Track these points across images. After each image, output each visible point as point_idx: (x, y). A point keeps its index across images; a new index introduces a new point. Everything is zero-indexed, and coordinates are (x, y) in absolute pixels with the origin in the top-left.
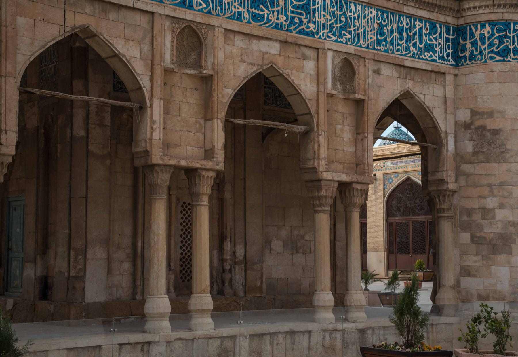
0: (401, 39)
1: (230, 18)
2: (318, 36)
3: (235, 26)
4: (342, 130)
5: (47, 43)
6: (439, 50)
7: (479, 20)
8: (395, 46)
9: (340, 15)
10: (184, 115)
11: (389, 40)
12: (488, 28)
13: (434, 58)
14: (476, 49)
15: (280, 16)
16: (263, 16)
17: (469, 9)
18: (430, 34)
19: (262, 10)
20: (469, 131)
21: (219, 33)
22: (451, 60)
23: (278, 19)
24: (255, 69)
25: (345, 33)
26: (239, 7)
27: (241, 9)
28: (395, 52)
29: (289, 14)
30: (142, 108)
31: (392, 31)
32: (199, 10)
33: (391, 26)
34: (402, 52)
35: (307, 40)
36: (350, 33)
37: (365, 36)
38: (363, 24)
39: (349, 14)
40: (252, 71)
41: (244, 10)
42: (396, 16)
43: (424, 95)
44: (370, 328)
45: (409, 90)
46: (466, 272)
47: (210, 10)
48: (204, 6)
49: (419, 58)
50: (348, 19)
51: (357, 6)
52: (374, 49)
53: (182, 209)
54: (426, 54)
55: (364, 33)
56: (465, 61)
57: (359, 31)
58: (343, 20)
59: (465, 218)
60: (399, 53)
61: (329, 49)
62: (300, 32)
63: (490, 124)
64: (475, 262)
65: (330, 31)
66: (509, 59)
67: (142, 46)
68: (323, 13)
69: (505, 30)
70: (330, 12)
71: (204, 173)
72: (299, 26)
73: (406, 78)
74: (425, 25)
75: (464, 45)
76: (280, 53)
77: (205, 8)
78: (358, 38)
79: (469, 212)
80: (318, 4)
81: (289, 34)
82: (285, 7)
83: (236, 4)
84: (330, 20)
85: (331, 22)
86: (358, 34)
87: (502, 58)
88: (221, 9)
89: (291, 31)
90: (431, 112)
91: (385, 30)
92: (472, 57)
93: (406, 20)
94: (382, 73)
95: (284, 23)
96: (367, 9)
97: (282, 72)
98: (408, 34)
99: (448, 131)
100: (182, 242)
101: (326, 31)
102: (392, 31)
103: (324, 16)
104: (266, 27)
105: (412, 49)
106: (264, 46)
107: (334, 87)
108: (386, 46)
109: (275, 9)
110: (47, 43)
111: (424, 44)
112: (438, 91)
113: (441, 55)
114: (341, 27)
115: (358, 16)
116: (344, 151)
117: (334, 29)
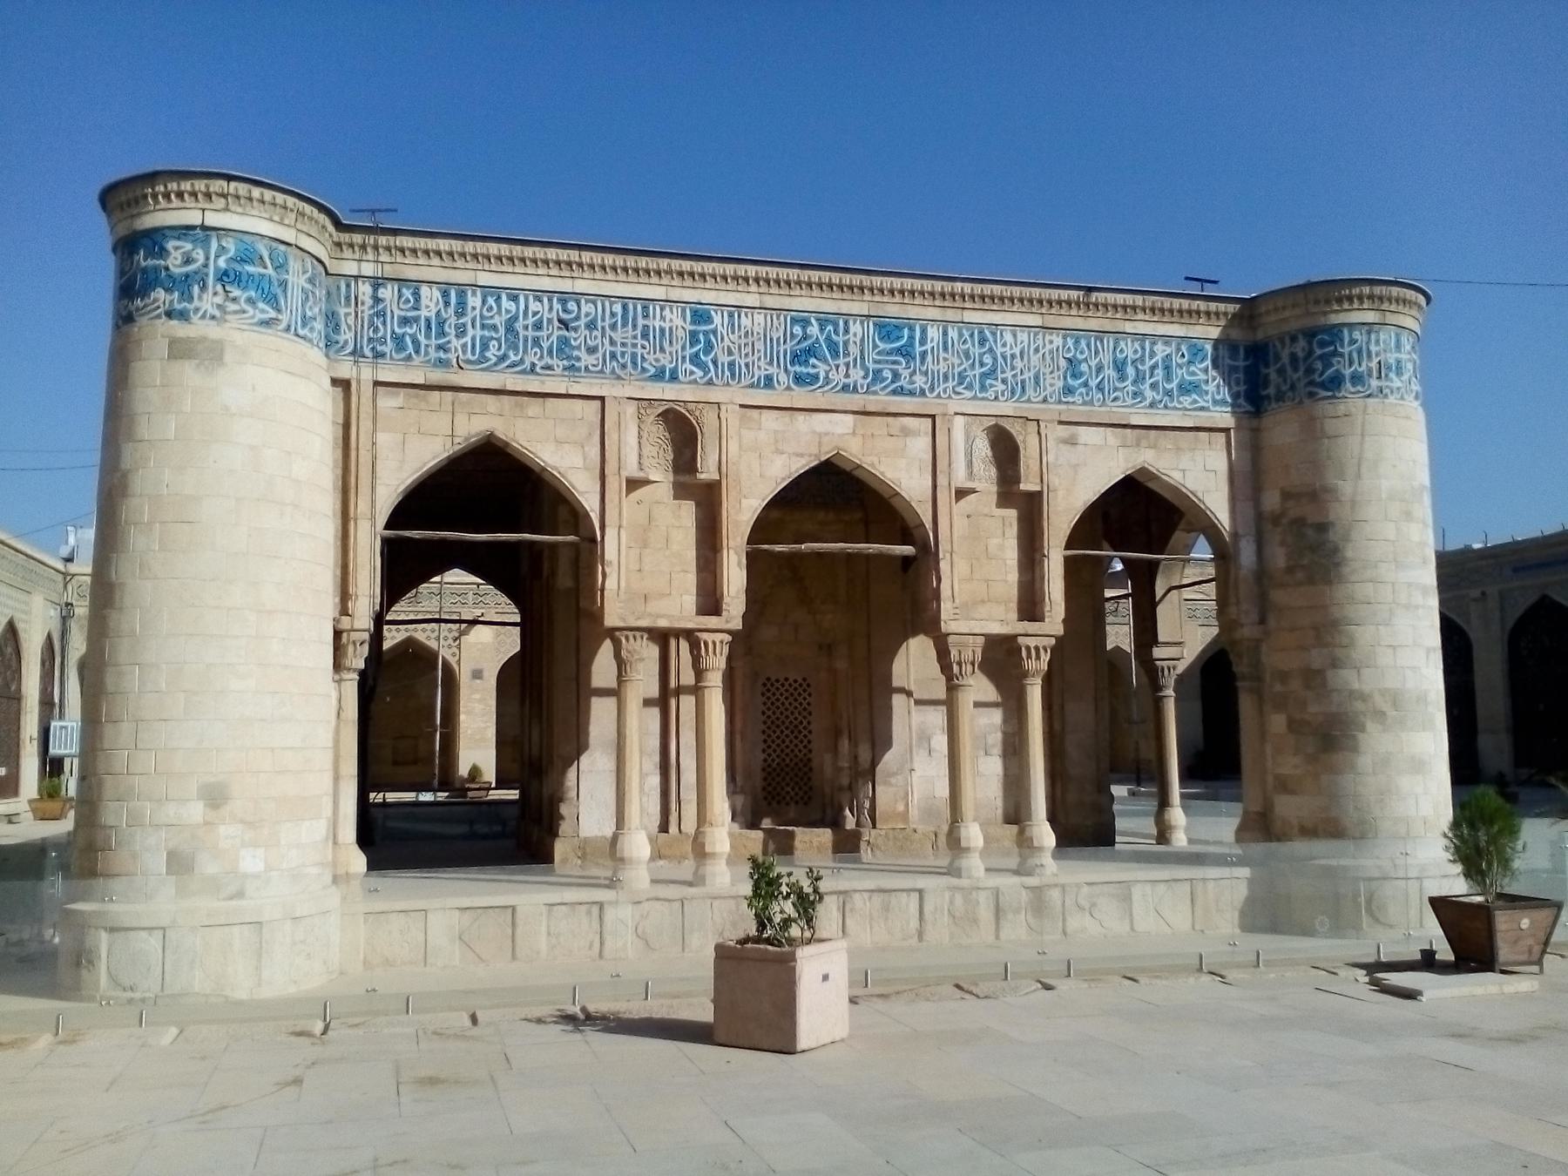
0: (1122, 378)
1: (752, 386)
2: (935, 394)
3: (761, 397)
4: (1001, 547)
5: (425, 464)
6: (1215, 389)
7: (1286, 328)
8: (1109, 393)
9: (981, 355)
10: (675, 547)
11: (1093, 383)
12: (1302, 342)
13: (1203, 404)
14: (1285, 381)
15: (851, 371)
16: (816, 377)
17: (1268, 312)
18: (1190, 362)
19: (814, 366)
20: (1279, 529)
22: (1244, 403)
23: (847, 376)
24: (803, 461)
25: (994, 382)
26: (767, 367)
27: (773, 370)
28: (1108, 402)
29: (871, 366)
31: (1100, 369)
32: (690, 383)
33: (1098, 360)
34: (1124, 401)
36: (1004, 381)
37: (1037, 383)
38: (1032, 364)
39: (999, 350)
40: (799, 465)
41: (778, 371)
42: (1108, 342)
43: (1184, 471)
44: (1056, 885)
45: (1146, 466)
46: (1284, 786)
47: (711, 379)
48: (701, 373)
49: (1166, 407)
50: (1000, 359)
51: (1019, 334)
52: (1060, 402)
53: (764, 690)
54: (1181, 399)
55: (1037, 378)
56: (1270, 403)
57: (1026, 376)
58: (988, 359)
59: (1278, 688)
60: (1119, 403)
61: (956, 414)
62: (894, 392)
64: (1296, 767)
65: (960, 384)
66: (1343, 393)
67: (586, 449)
68: (942, 355)
69: (1332, 343)
70: (958, 352)
71: (704, 636)
72: (893, 382)
73: (1138, 445)
74: (1178, 349)
75: (1267, 375)
76: (854, 431)
77: (700, 378)
78: (1023, 388)
79: (1284, 677)
80: (932, 341)
81: (872, 397)
82: (862, 352)
83: (762, 363)
84: (959, 365)
85: (963, 367)
86: (1023, 382)
87: (1330, 394)
88: (733, 375)
89: (875, 393)
90: (1199, 500)
91: (1084, 367)
92: (1280, 397)
93: (1133, 345)
94: (1081, 440)
95: (860, 381)
96: (1040, 336)
97: (858, 462)
98: (1137, 368)
99: (1241, 531)
100: (765, 741)
101: (950, 384)
102: (1100, 369)
103: (945, 359)
104: (823, 393)
105: (1149, 394)
106: (821, 422)
107: (971, 474)
108: (1087, 394)
109: (841, 361)
110: (425, 464)
111: (1176, 382)
113: (1218, 397)
114: (984, 376)
115: (1022, 353)
116: (1006, 581)
117: (968, 379)
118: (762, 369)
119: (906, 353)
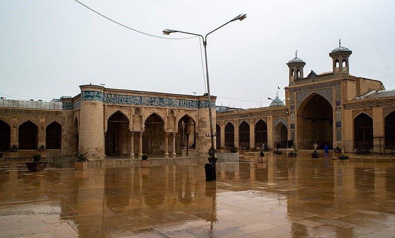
3: (147, 106)
21: (144, 108)
30: (129, 122)
35: (163, 107)
63: (204, 120)
112: (195, 114)
118: (147, 104)
119: (162, 101)
